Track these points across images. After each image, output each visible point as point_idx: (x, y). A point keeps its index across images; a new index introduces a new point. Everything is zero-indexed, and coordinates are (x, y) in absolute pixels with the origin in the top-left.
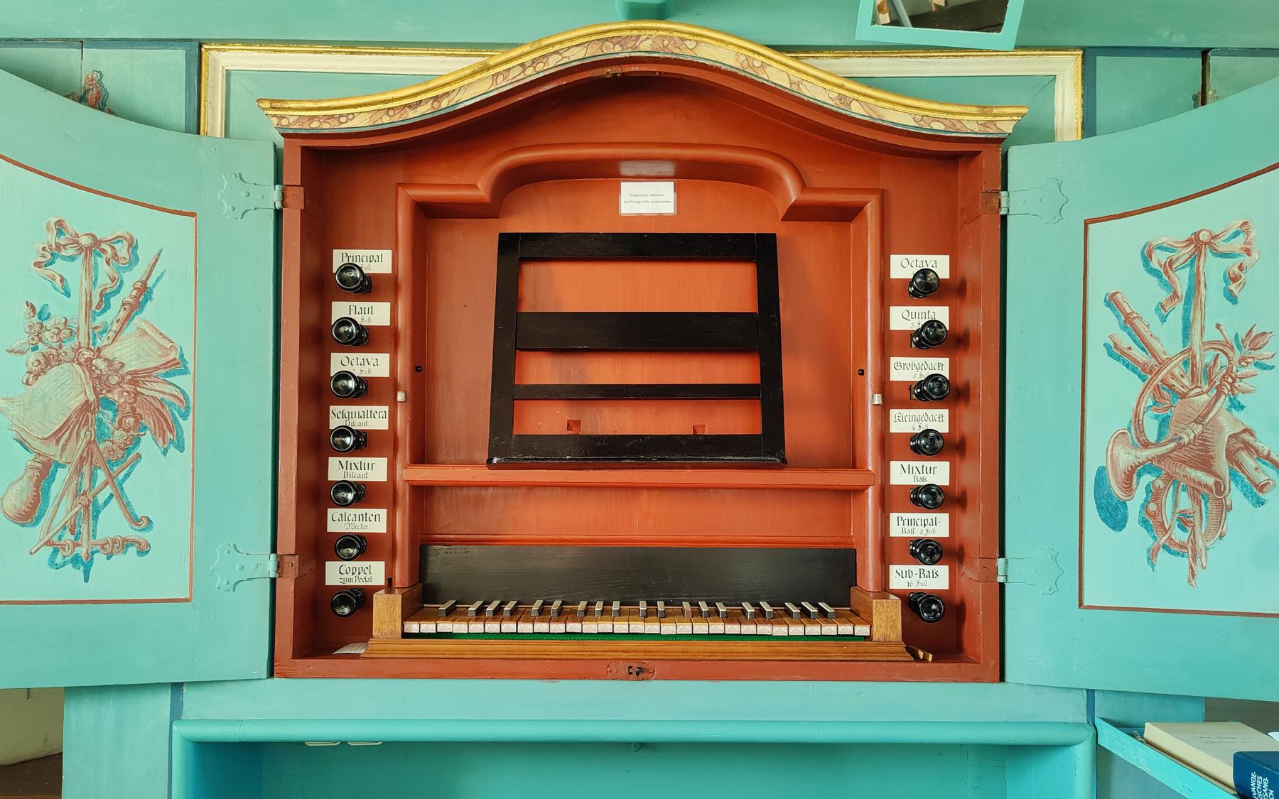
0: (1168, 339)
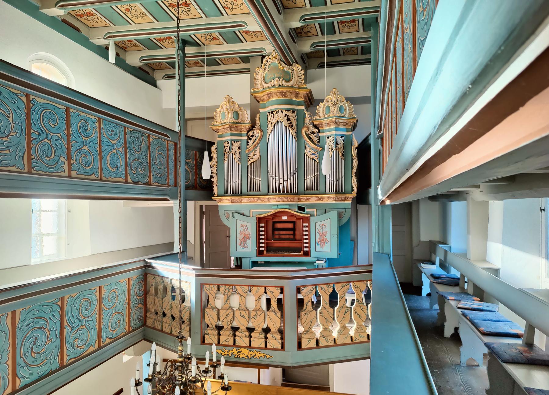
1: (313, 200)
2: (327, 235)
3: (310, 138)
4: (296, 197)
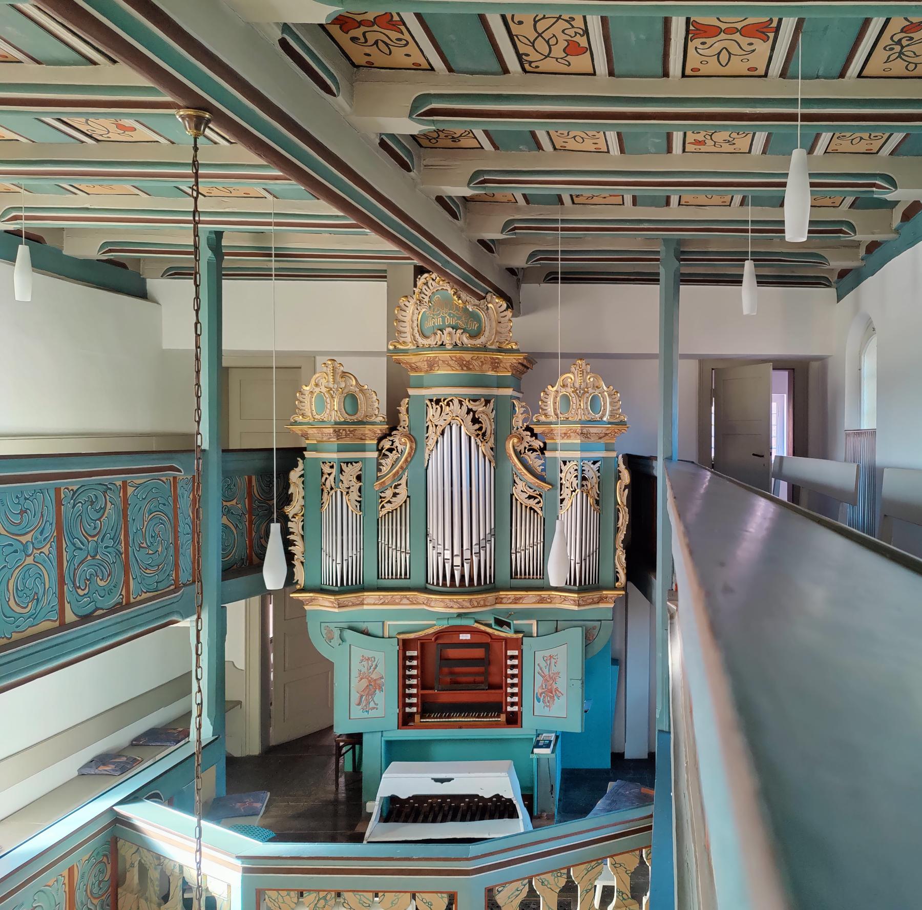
0: (547, 673)
1: (529, 600)
2: (558, 680)
4: (491, 597)
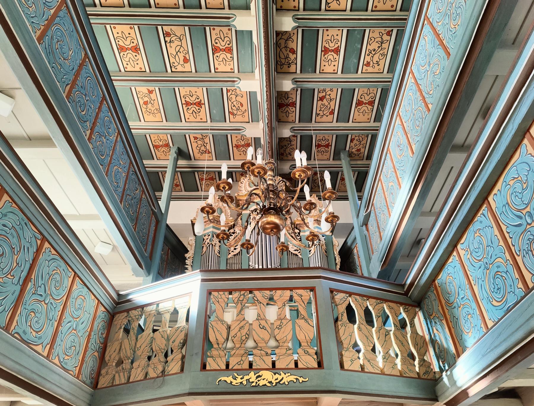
3: (292, 237)
